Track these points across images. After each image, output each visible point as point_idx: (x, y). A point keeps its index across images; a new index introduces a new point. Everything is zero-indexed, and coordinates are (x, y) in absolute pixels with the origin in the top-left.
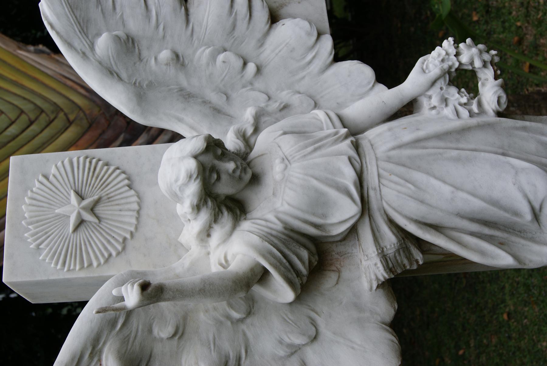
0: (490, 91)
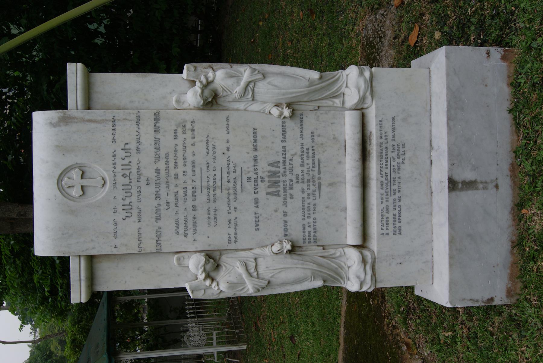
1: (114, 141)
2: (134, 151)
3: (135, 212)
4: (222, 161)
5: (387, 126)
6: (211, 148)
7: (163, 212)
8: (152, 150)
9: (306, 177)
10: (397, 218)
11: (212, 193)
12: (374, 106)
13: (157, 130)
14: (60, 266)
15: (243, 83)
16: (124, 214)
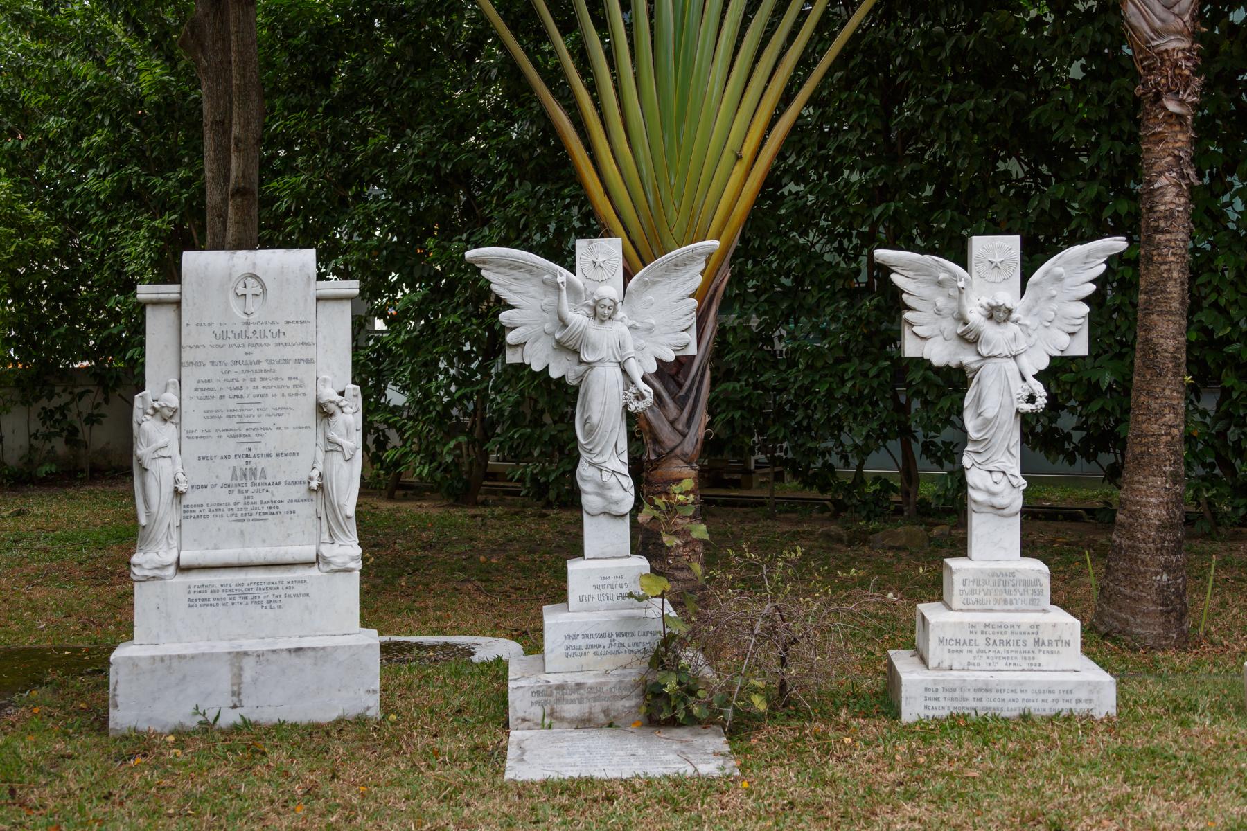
0: (1028, 407)
1: (287, 322)
2: (277, 340)
3: (221, 342)
4: (267, 422)
5: (299, 589)
6: (280, 412)
7: (219, 368)
8: (278, 357)
9: (250, 507)
10: (205, 603)
11: (236, 413)
12: (320, 574)
13: (296, 361)
14: (171, 273)
15: (339, 440)
16: (218, 332)
